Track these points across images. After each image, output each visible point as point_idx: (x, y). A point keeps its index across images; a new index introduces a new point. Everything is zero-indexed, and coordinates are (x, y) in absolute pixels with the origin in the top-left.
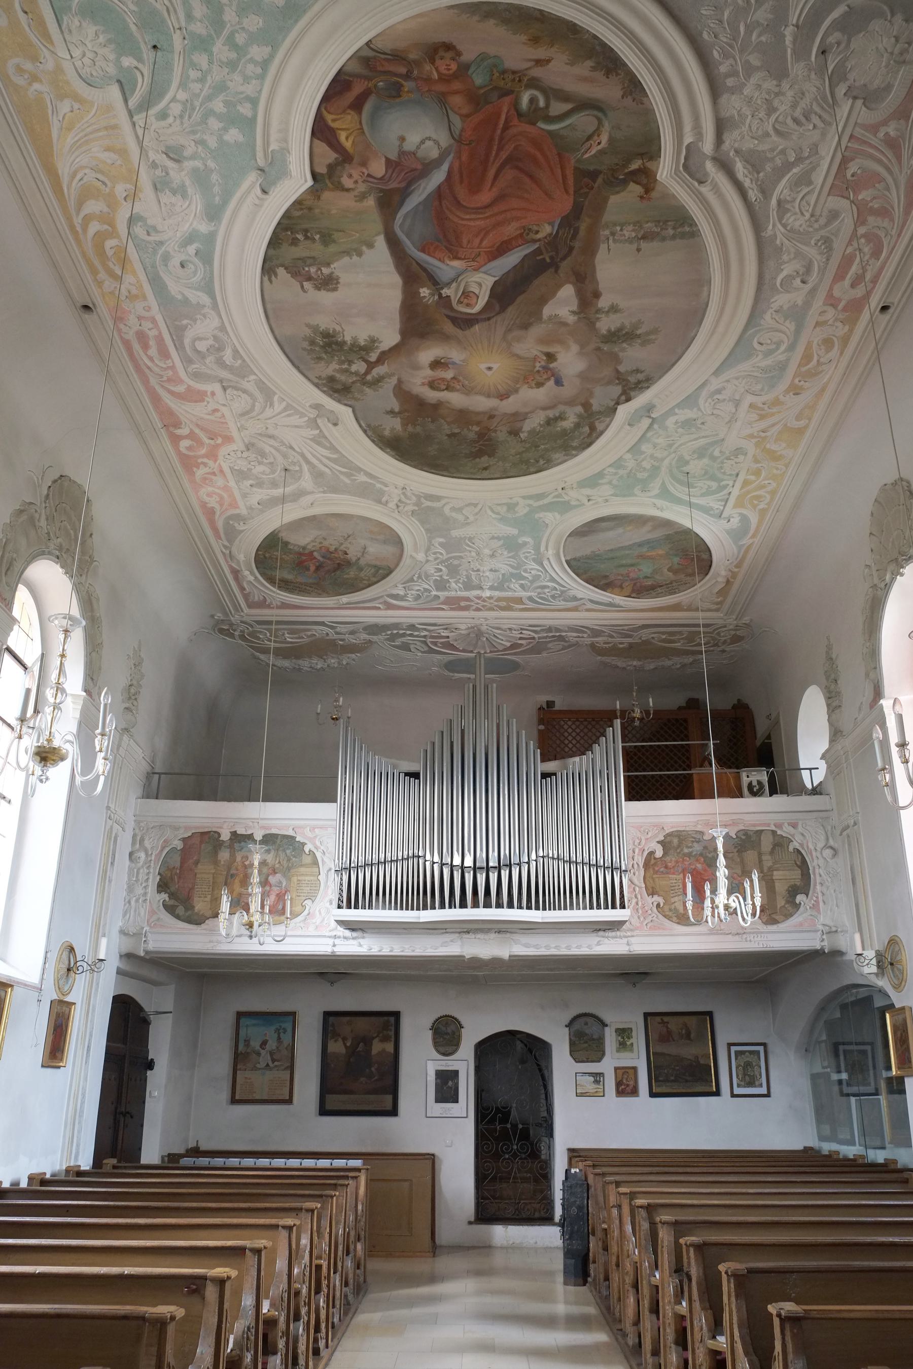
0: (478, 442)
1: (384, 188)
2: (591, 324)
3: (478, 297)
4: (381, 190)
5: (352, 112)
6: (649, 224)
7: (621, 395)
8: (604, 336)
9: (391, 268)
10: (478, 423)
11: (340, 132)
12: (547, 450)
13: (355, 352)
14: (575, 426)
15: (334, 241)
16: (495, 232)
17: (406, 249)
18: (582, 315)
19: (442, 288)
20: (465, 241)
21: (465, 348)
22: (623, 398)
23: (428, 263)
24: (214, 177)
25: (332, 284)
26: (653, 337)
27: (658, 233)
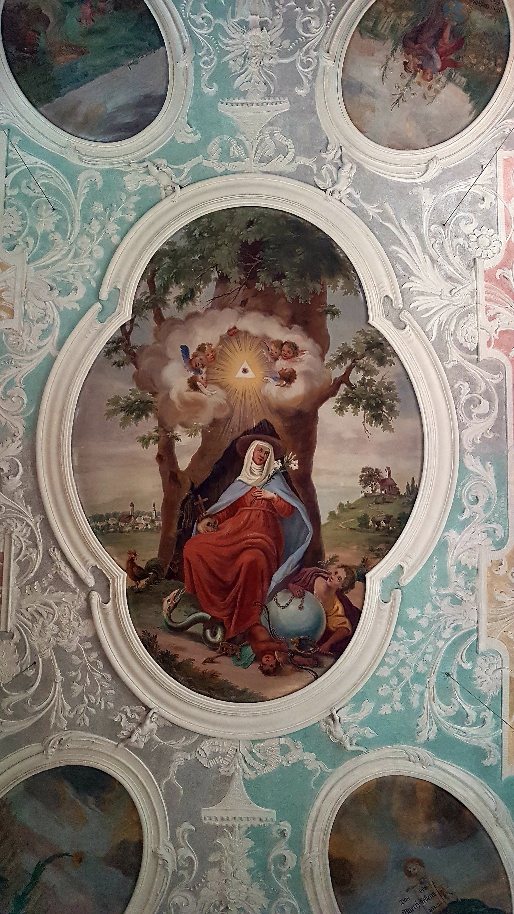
0: (256, 266)
1: (317, 568)
2: (162, 424)
3: (253, 459)
4: (318, 565)
5: (332, 629)
6: (127, 529)
7: (130, 332)
8: (151, 410)
9: (318, 491)
10: (256, 294)
11: (342, 614)
12: (193, 253)
13: (357, 396)
14: (168, 288)
15: (358, 519)
16: (240, 525)
17: (305, 510)
18: (170, 434)
19: (281, 469)
20: (262, 517)
21: (265, 397)
22: (128, 328)
23: (291, 496)
24: (433, 581)
25: (366, 475)
26: (111, 407)
27: (119, 521)
